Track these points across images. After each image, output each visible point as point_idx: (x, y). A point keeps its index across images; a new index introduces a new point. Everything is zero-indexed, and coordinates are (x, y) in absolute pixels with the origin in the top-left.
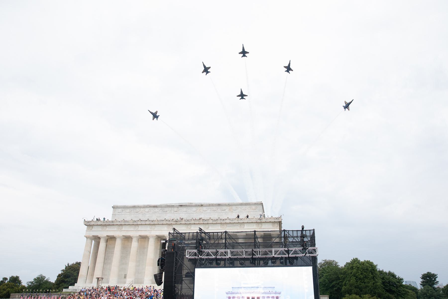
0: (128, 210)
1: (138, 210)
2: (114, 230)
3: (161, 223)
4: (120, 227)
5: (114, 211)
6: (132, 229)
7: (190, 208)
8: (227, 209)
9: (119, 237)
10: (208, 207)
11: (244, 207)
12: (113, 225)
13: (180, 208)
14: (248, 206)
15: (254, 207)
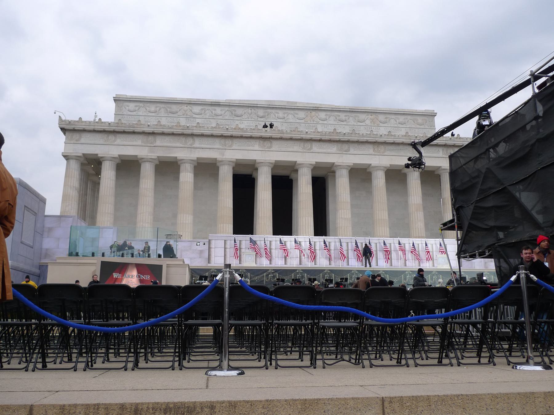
0: (153, 108)
1: (174, 108)
2: (134, 143)
3: (249, 134)
4: (151, 138)
5: (118, 108)
6: (178, 145)
7: (292, 112)
8: (367, 119)
9: (150, 160)
10: (329, 113)
11: (402, 119)
12: (134, 133)
13: (269, 111)
14: (409, 117)
15: (420, 120)
